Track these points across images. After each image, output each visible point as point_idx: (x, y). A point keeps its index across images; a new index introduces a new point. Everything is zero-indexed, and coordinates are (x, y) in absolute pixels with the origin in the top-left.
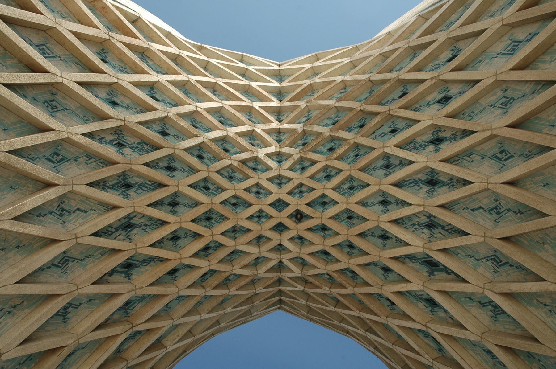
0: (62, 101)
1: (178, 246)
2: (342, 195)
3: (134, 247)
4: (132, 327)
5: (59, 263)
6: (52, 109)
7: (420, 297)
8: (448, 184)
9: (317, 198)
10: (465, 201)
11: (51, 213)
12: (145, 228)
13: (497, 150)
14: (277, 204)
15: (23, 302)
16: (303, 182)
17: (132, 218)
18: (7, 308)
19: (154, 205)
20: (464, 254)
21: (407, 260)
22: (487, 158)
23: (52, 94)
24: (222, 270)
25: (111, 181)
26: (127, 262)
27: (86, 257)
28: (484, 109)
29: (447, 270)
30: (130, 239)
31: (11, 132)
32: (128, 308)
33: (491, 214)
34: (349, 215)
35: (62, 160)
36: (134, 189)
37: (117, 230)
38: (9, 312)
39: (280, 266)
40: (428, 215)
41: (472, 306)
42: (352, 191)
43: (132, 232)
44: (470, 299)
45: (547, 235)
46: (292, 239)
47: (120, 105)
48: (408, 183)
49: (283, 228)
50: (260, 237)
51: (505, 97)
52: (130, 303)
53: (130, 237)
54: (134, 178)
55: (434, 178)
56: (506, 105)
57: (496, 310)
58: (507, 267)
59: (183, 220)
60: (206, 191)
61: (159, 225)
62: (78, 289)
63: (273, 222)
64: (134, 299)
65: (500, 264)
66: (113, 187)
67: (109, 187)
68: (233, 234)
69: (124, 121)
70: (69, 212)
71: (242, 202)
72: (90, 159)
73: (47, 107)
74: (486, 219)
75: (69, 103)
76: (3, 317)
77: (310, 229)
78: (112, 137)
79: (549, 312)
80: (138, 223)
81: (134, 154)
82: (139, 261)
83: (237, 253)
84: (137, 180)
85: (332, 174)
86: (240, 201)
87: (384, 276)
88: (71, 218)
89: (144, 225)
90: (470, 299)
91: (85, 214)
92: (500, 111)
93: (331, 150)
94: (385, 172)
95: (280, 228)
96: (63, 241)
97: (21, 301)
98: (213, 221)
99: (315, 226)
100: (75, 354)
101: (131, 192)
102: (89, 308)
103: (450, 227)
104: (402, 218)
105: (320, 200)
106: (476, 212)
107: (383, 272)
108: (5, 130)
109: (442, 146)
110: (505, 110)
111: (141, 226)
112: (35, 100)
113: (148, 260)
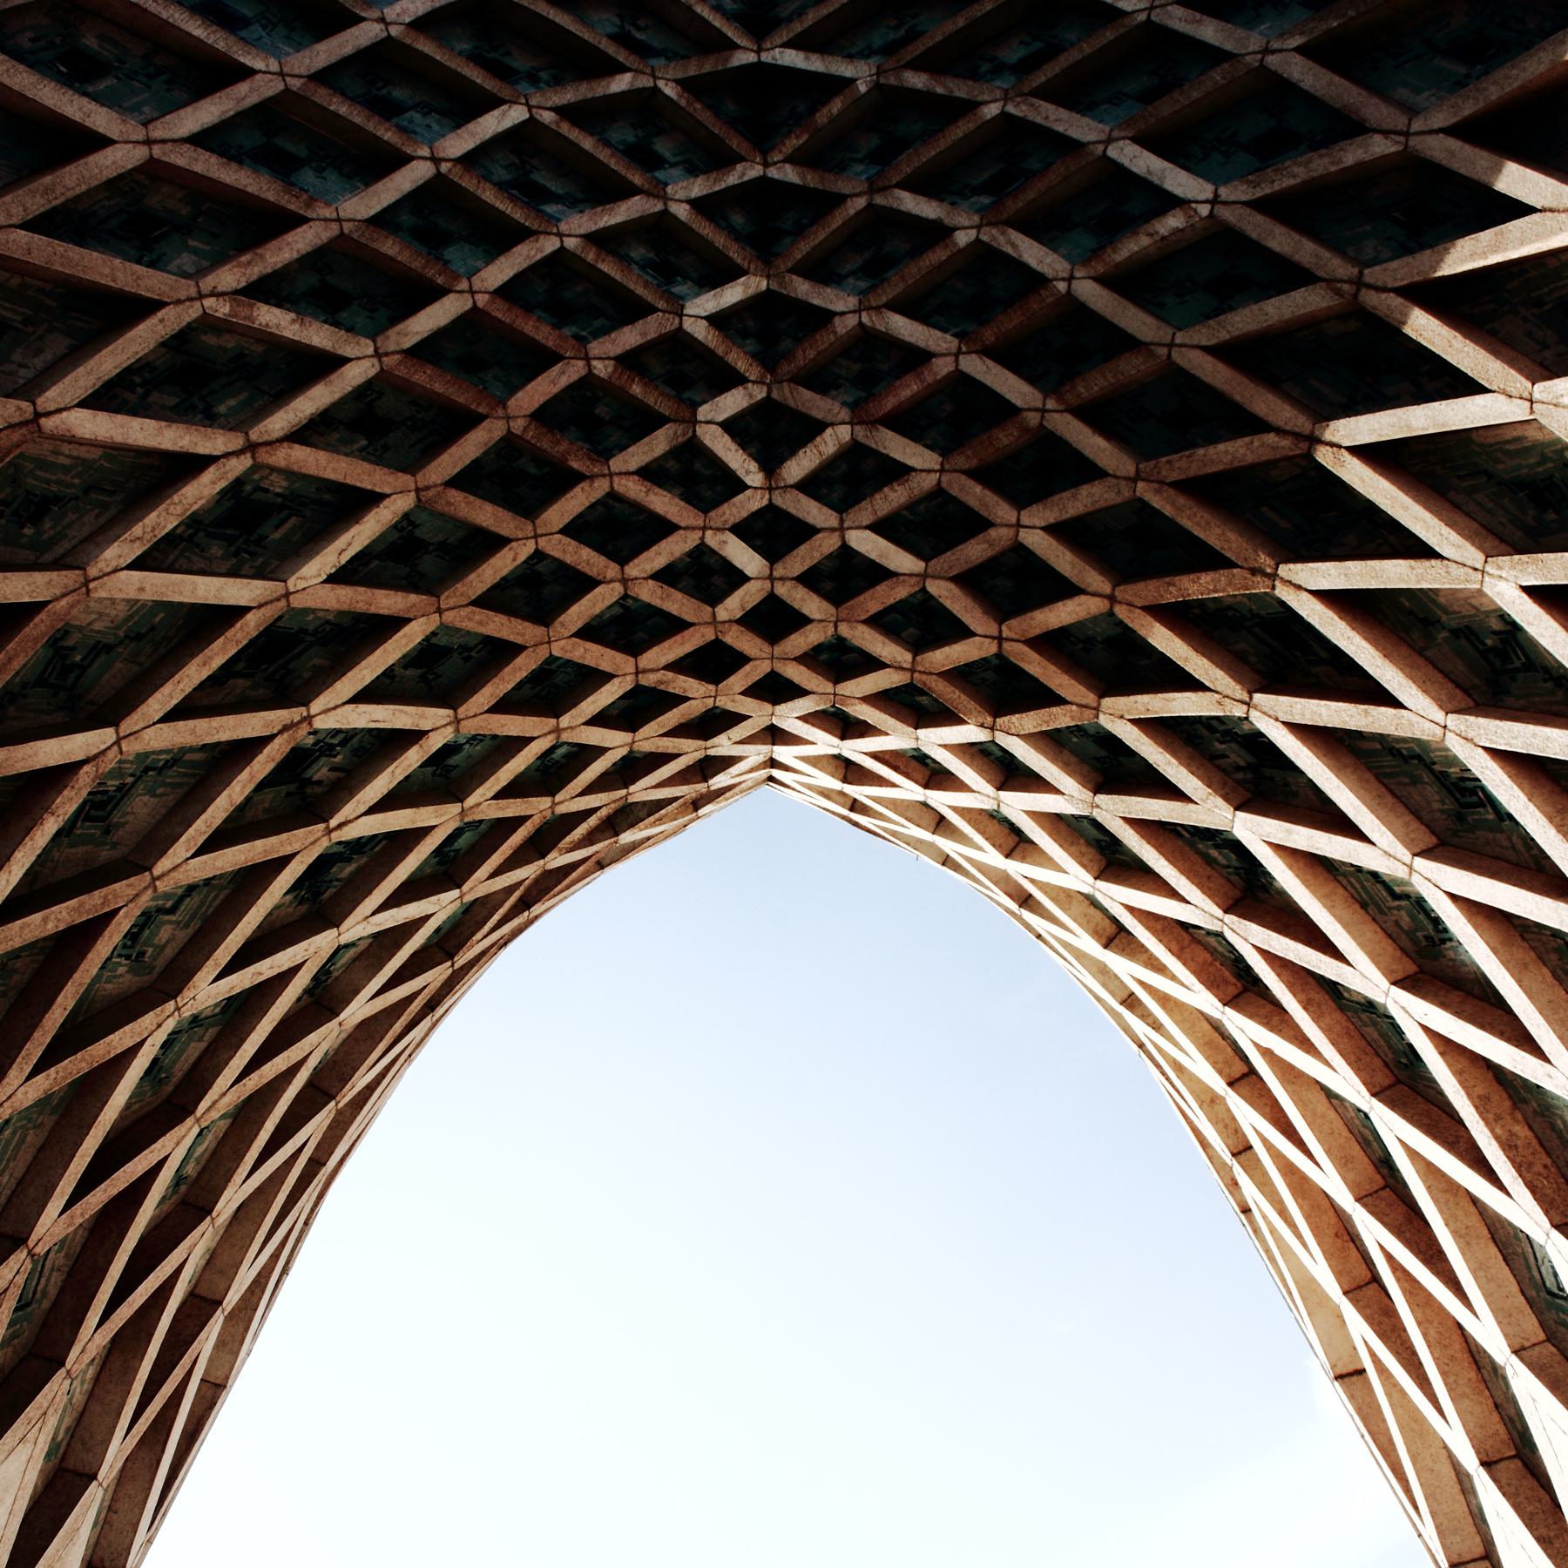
39: (771, 434)
40: (309, 791)
46: (738, 578)
54: (1224, 862)
59: (1088, 713)
63: (800, 641)
80: (1234, 745)
84: (1214, 853)
95: (773, 620)
107: (418, 533)
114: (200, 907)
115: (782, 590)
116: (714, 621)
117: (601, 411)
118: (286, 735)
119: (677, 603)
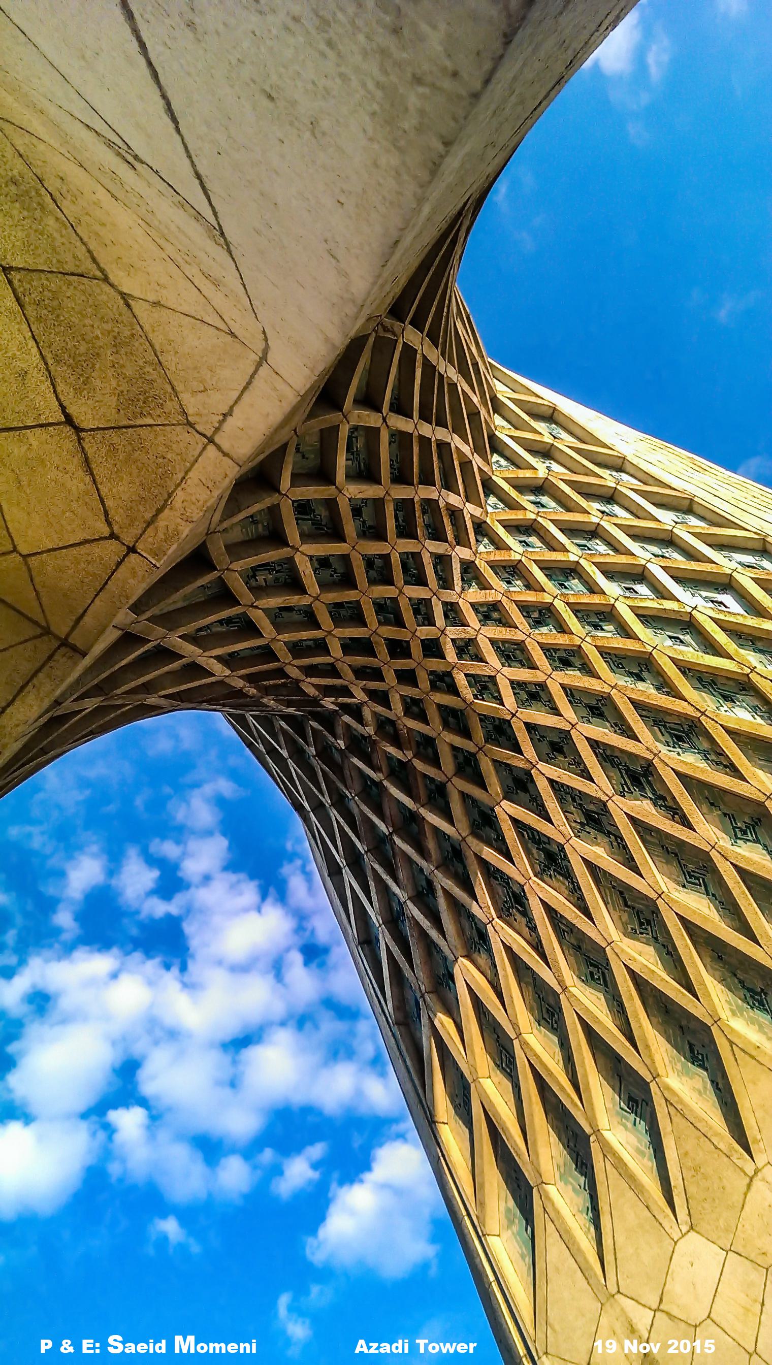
4: (703, 713)
5: (700, 885)
11: (656, 939)
16: (354, 678)
17: (581, 823)
26: (633, 785)
35: (592, 965)
36: (547, 846)
37: (609, 833)
41: (312, 446)
43: (595, 809)
52: (676, 736)
64: (666, 734)
67: (573, 883)
68: (490, 685)
72: (564, 931)
78: (518, 916)
82: (619, 770)
83: (503, 651)
84: (534, 851)
98: (497, 723)
101: (555, 848)
102: (722, 800)
111: (580, 804)
119: (408, 615)
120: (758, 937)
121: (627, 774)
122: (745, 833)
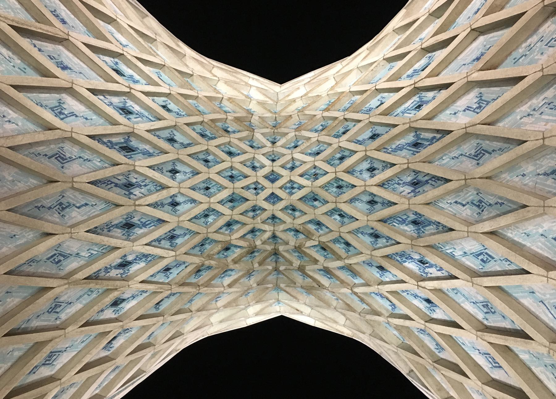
0: (477, 312)
1: (369, 161)
2: (215, 210)
3: (410, 165)
4: (415, 83)
5: (484, 154)
6: (487, 305)
7: (138, 116)
8: (114, 225)
9: (238, 206)
10: (95, 212)
11: (490, 205)
12: (400, 182)
13: (64, 263)
14: (276, 199)
15: (521, 119)
16: (252, 220)
17: (412, 191)
18: (537, 114)
19: (392, 204)
20: (94, 161)
21: (151, 151)
22: (74, 255)
23: (487, 319)
24: (328, 137)
25: (431, 229)
26: (417, 149)
27: (457, 158)
28: (78, 299)
29: (111, 145)
30: (414, 171)
31: (527, 289)
32: (418, 102)
33: (68, 203)
34: (208, 191)
35: (479, 255)
36: (409, 219)
37: (427, 182)
38: (534, 110)
40: (132, 196)
42: (206, 213)
43: (412, 178)
44: (86, 119)
45: (10, 189)
46: (263, 166)
47: (423, 299)
48: (152, 224)
49: (271, 177)
50: (292, 168)
51: (57, 313)
52: (416, 108)
53: (414, 173)
55: (126, 230)
56: (56, 305)
57: (59, 110)
58: (50, 154)
60: (342, 213)
61: (386, 183)
62: (466, 128)
65: (58, 156)
66: (430, 223)
68: (317, 172)
69: (418, 285)
70: (472, 203)
71: (308, 202)
72: (451, 253)
73: (492, 308)
74: (73, 197)
75: (471, 308)
76: (540, 105)
77: (246, 177)
79: (5, 115)
80: (407, 186)
81: (409, 253)
82: (405, 149)
84: (406, 228)
85: (225, 228)
86: (311, 203)
87: (173, 134)
88: (471, 198)
89: (400, 184)
90: (86, 119)
91: (457, 200)
92: (62, 299)
93: (227, 249)
94: (175, 233)
96: (479, 178)
97: (522, 120)
98: (335, 185)
99: (241, 180)
100: (472, 59)
101: (412, 217)
102: (457, 106)
103: (109, 186)
104: (158, 191)
105: (236, 204)
106: (83, 203)
107: (175, 138)
108: (533, 292)
109: (119, 261)
110: (57, 300)
111: (403, 183)
112: (504, 317)
113: (398, 149)
114: (89, 212)
115: (275, 169)
116: (256, 176)
117: (229, 129)
118: (126, 166)
120: (521, 139)
121: (409, 146)
122: (480, 107)
